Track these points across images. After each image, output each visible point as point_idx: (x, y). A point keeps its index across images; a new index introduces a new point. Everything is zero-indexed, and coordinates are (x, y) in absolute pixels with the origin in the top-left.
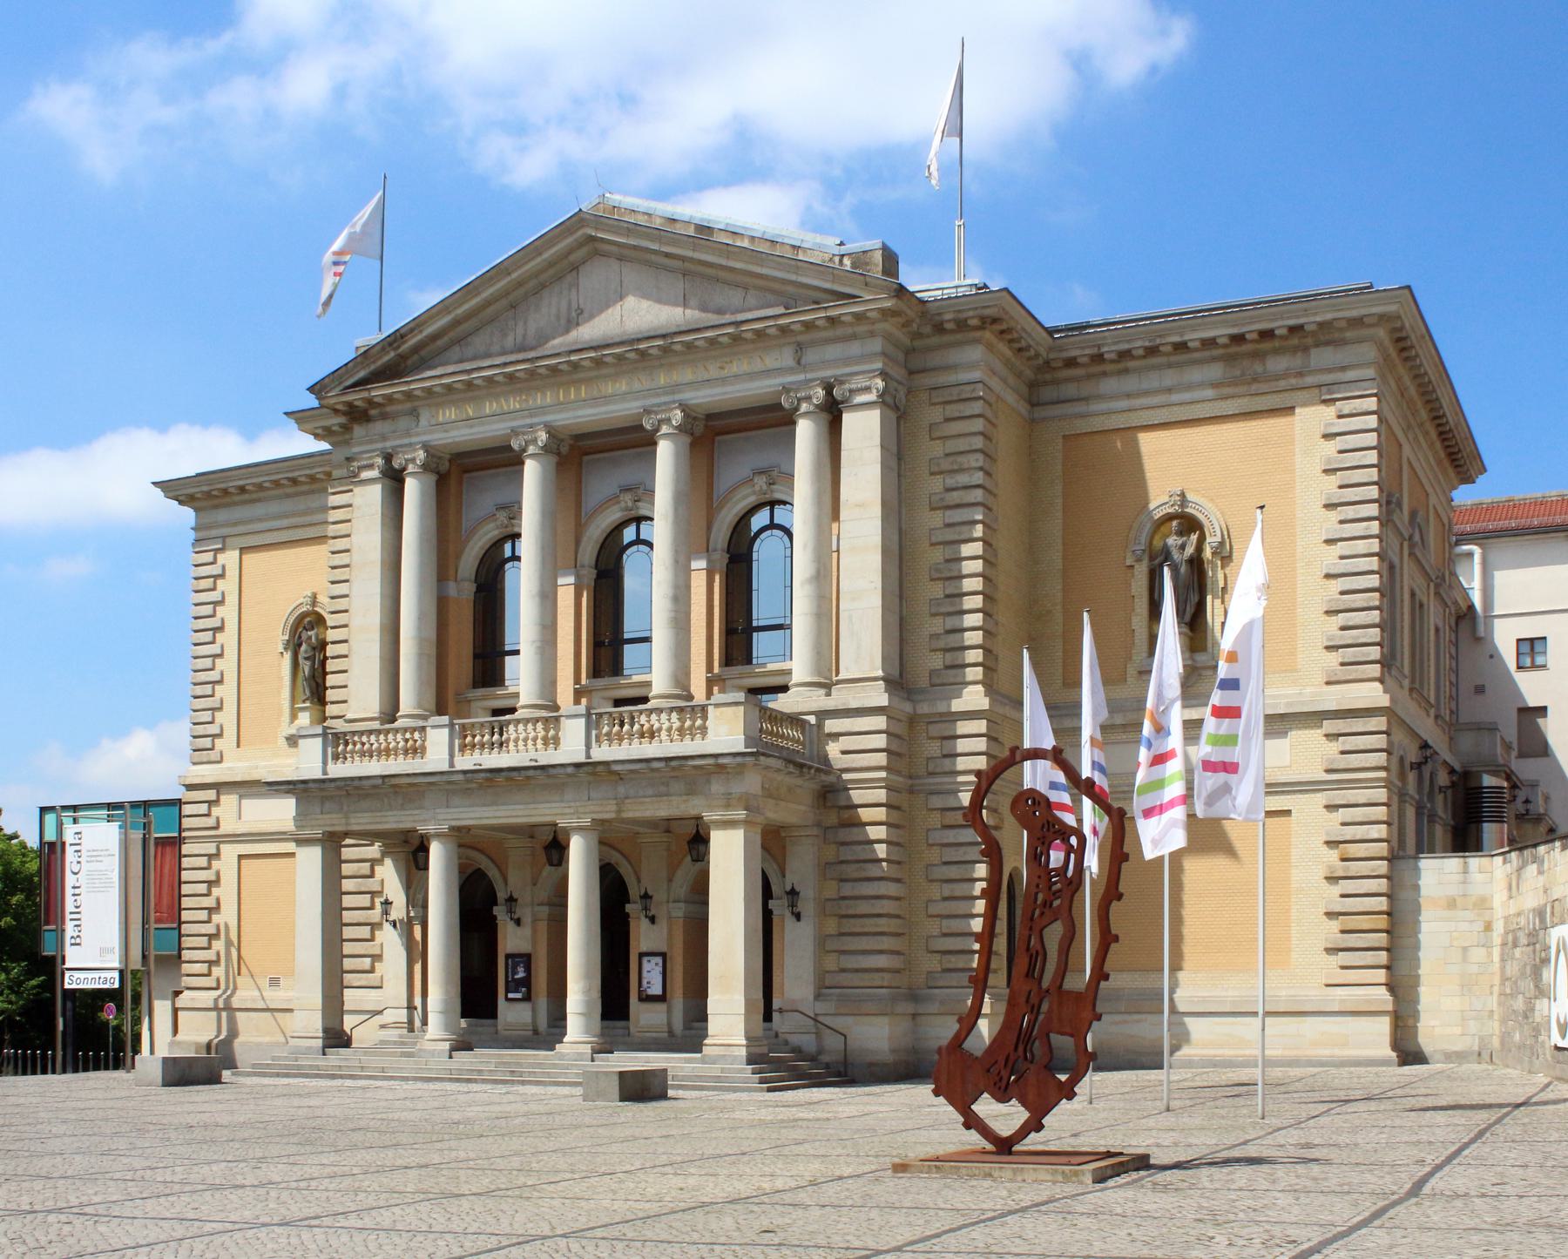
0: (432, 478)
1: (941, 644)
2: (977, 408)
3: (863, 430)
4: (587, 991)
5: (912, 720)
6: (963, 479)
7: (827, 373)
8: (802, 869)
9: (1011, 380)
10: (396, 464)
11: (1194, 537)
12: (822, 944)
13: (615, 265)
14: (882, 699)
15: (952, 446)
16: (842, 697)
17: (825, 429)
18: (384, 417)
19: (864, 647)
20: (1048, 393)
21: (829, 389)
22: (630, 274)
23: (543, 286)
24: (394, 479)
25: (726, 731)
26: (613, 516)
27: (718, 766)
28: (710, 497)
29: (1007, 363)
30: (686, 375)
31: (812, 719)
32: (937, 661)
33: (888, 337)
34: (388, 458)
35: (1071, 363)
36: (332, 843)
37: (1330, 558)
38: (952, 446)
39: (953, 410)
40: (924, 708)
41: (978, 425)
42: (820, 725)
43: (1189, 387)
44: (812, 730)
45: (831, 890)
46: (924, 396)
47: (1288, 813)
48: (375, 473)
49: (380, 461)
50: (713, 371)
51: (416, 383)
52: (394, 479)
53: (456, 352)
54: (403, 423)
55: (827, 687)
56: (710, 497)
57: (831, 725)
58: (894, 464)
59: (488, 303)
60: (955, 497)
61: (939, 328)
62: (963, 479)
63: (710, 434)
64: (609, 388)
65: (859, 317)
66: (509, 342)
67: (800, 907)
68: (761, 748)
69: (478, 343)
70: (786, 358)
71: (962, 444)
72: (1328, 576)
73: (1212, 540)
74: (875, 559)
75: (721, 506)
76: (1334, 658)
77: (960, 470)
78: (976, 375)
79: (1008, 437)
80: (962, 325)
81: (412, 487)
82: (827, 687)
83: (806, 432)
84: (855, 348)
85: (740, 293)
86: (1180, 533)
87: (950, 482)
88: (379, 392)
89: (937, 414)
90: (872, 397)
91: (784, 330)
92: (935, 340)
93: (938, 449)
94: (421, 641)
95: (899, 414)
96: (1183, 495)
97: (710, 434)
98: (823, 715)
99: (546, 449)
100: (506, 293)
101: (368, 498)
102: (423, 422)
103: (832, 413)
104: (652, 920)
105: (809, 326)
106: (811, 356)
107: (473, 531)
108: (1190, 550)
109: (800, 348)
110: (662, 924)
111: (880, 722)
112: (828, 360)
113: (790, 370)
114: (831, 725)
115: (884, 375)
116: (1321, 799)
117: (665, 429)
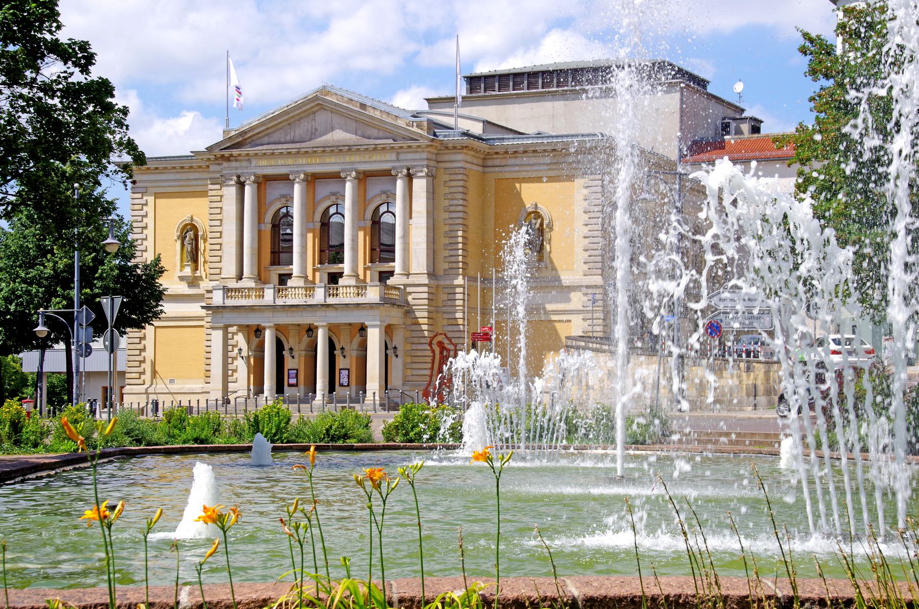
0: (256, 185)
1: (448, 260)
2: (460, 177)
3: (420, 185)
4: (324, 382)
5: (437, 287)
6: (456, 202)
7: (408, 164)
8: (398, 340)
9: (475, 161)
10: (242, 179)
11: (539, 221)
12: (405, 366)
13: (330, 114)
14: (427, 282)
15: (452, 190)
16: (412, 280)
17: (407, 182)
18: (236, 160)
19: (419, 262)
20: (490, 163)
21: (408, 169)
22: (336, 119)
23: (301, 118)
24: (241, 185)
25: (373, 294)
26: (328, 203)
27: (371, 306)
28: (365, 200)
29: (473, 156)
30: (358, 159)
31: (402, 287)
32: (446, 266)
33: (429, 152)
34: (239, 177)
35: (497, 153)
36: (225, 328)
37: (585, 230)
38: (452, 190)
39: (453, 177)
40: (442, 283)
41: (461, 183)
42: (405, 289)
43: (540, 164)
44: (403, 291)
45: (409, 347)
46: (442, 171)
47: (570, 321)
48: (233, 182)
49: (235, 178)
50: (367, 158)
51: (251, 150)
52: (241, 185)
53: (266, 140)
54: (245, 164)
55: (408, 275)
56: (365, 200)
57: (409, 289)
58: (431, 196)
59: (280, 123)
60: (452, 208)
61: (447, 148)
62: (456, 202)
63: (364, 177)
64: (328, 160)
65: (419, 146)
66: (288, 138)
67: (398, 353)
68: (386, 301)
69: (275, 137)
70: (393, 156)
71: (455, 190)
72: (585, 237)
73: (546, 222)
74: (424, 232)
75: (369, 204)
76: (586, 267)
77: (455, 199)
78: (460, 165)
79: (472, 184)
80: (455, 148)
81: (248, 189)
82: (408, 275)
83: (400, 184)
84: (417, 156)
85: (376, 131)
86: (535, 219)
87: (451, 203)
88: (235, 152)
89: (447, 178)
90: (423, 174)
91: (393, 148)
92: (446, 151)
93: (447, 190)
94: (252, 248)
95: (431, 177)
96: (536, 205)
97: (364, 177)
98: (406, 286)
99: (303, 180)
100: (287, 120)
101: (230, 192)
102: (253, 165)
103: (410, 177)
104: (344, 357)
105: (401, 147)
106: (402, 157)
107: (271, 204)
108: (538, 226)
109: (398, 154)
110: (348, 357)
111: (426, 289)
112: (408, 158)
113: (394, 161)
114: (409, 289)
115: (428, 167)
116: (581, 316)
117: (349, 178)
